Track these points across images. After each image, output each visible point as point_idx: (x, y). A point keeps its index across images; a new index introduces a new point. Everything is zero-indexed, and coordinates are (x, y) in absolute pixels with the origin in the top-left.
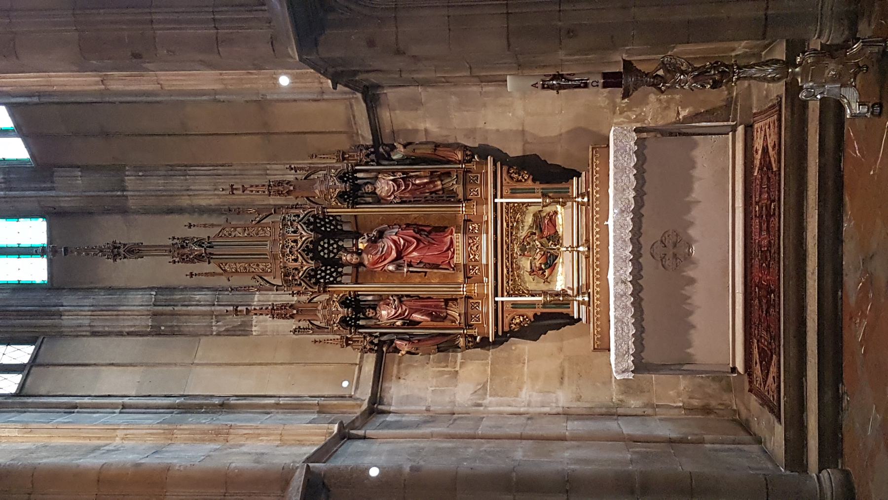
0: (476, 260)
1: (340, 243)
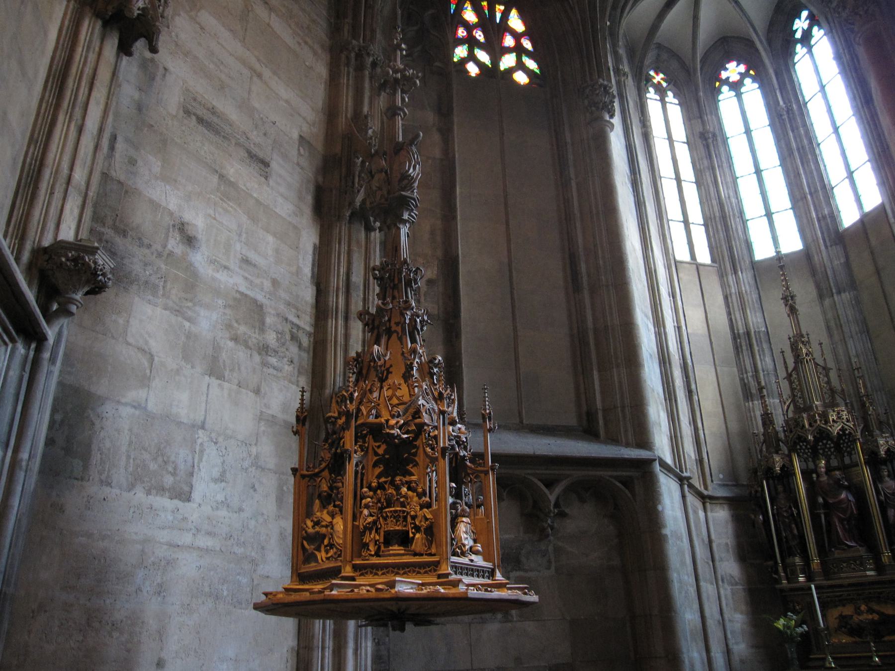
0: (842, 568)
1: (833, 457)
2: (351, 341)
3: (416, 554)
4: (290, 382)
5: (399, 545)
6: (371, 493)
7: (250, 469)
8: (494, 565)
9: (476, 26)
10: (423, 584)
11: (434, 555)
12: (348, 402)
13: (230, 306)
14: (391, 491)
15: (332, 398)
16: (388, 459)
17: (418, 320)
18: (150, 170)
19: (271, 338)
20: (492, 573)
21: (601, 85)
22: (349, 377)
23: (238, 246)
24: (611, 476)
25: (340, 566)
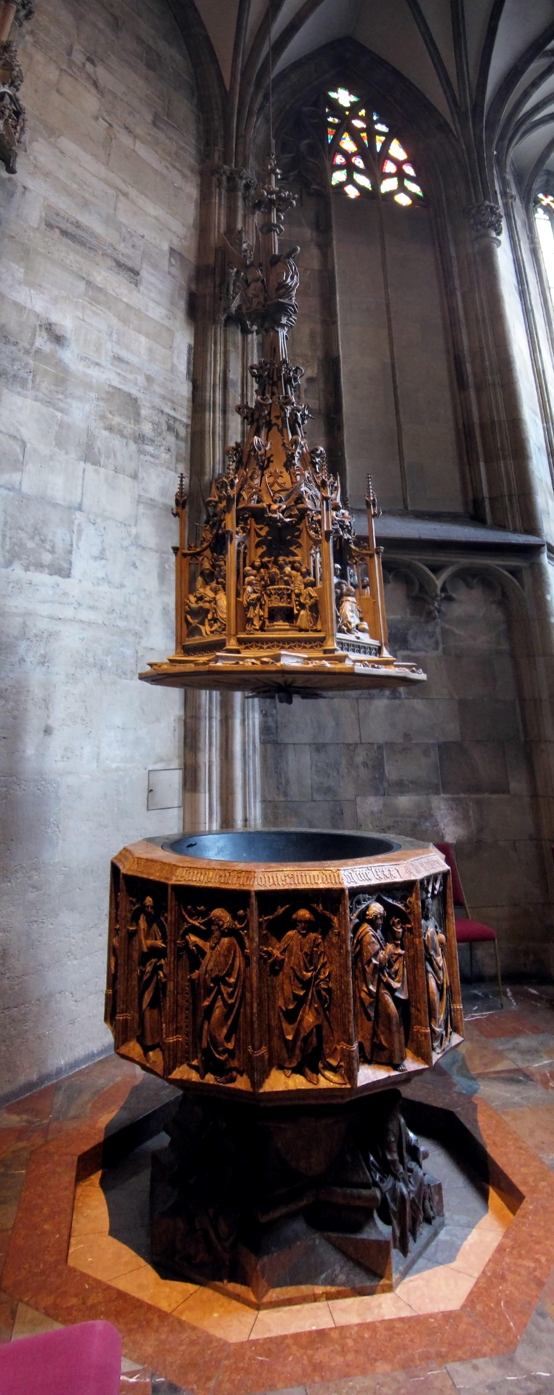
2: (230, 432)
3: (301, 630)
4: (168, 468)
5: (284, 621)
6: (254, 572)
7: (130, 548)
8: (381, 642)
9: (354, 154)
10: (309, 659)
11: (320, 631)
12: (229, 488)
13: (103, 399)
14: (275, 570)
15: (211, 483)
16: (270, 540)
17: (299, 414)
18: (13, 276)
19: (147, 428)
20: (379, 651)
21: (488, 206)
22: (229, 465)
23: (109, 345)
24: (498, 565)
25: (225, 640)
